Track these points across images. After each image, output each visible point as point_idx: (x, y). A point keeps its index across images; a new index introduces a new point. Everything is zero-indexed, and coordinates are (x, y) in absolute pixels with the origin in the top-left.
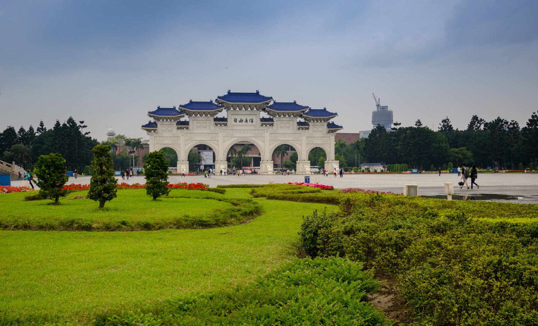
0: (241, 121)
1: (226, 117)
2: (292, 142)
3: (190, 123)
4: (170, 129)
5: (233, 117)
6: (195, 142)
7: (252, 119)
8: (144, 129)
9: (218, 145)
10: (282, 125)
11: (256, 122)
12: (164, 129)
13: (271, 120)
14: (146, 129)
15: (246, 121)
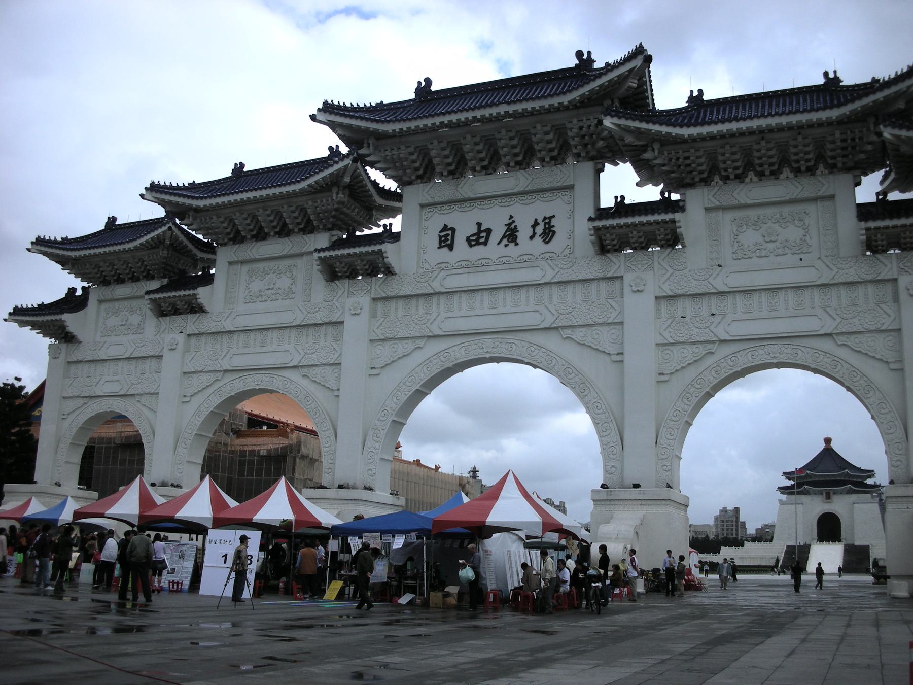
0: (480, 237)
1: (396, 228)
2: (827, 345)
3: (219, 284)
4: (135, 319)
5: (437, 221)
6: (228, 378)
7: (548, 221)
8: (22, 324)
9: (335, 393)
10: (750, 237)
11: (571, 235)
12: (113, 321)
13: (677, 207)
14: (34, 326)
15: (511, 235)
